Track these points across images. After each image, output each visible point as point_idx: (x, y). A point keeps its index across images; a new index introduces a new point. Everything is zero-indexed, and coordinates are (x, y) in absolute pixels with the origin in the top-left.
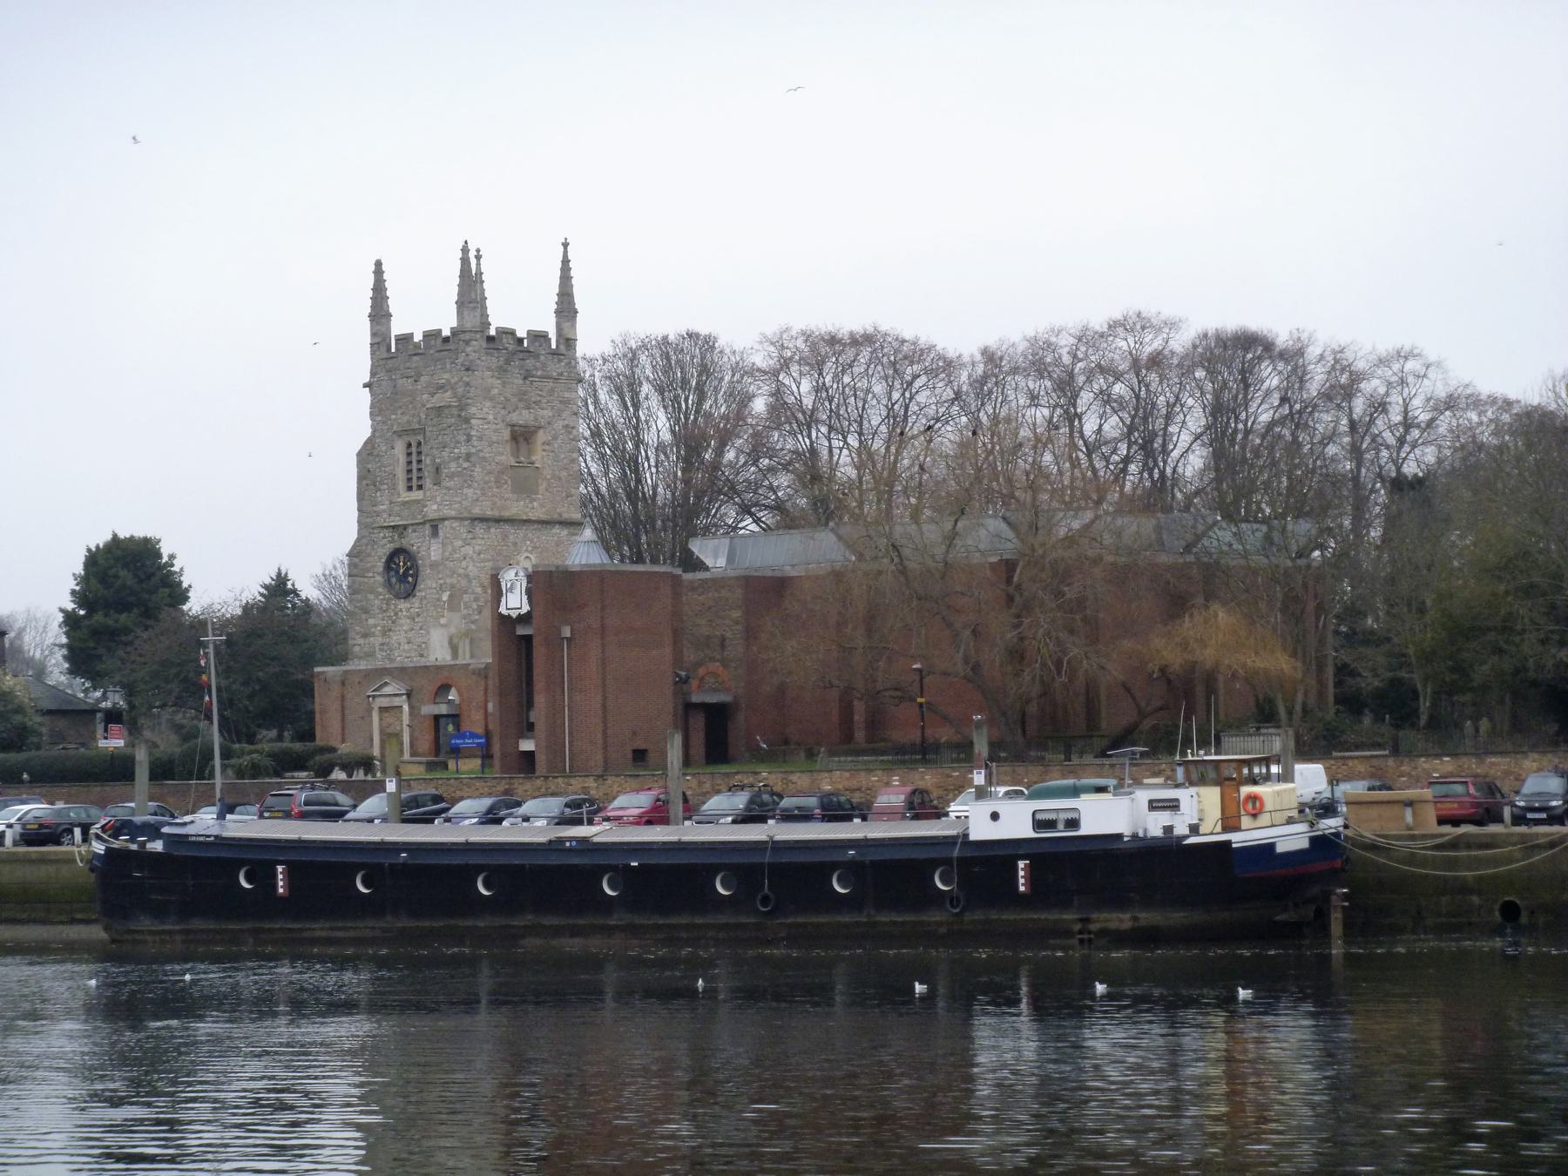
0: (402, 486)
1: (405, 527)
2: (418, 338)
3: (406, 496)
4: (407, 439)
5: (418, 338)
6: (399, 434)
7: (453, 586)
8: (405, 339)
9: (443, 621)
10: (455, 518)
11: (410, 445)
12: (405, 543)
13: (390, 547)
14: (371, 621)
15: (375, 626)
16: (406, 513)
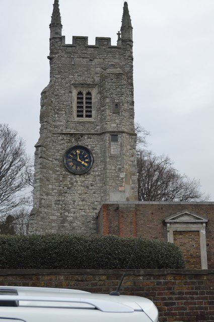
0: (75, 114)
1: (82, 135)
2: (92, 42)
3: (77, 119)
4: (79, 89)
5: (92, 42)
6: (75, 85)
7: (127, 170)
8: (80, 41)
9: (120, 189)
10: (127, 133)
11: (80, 93)
12: (80, 144)
13: (67, 146)
14: (50, 186)
15: (53, 190)
16: (81, 128)
